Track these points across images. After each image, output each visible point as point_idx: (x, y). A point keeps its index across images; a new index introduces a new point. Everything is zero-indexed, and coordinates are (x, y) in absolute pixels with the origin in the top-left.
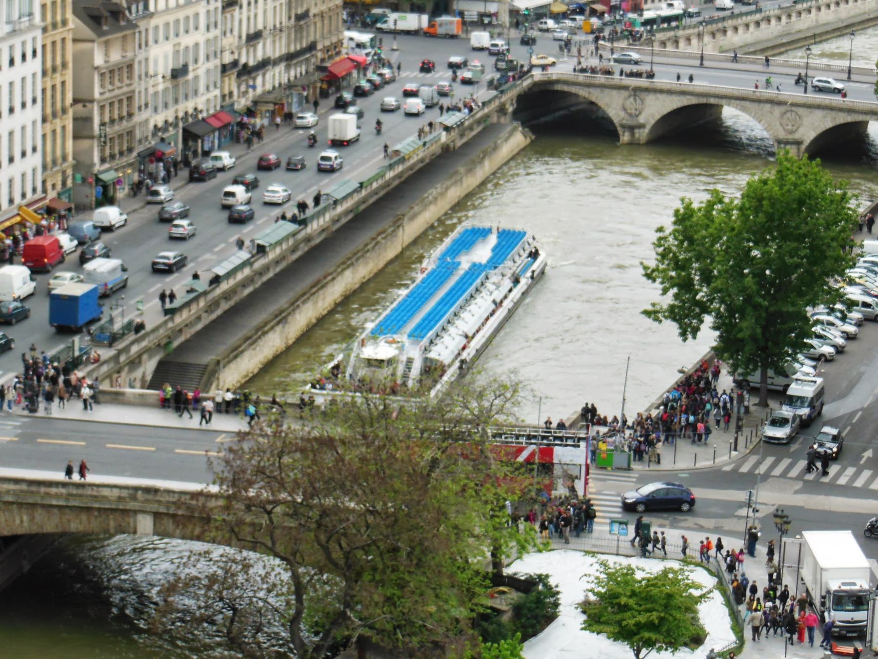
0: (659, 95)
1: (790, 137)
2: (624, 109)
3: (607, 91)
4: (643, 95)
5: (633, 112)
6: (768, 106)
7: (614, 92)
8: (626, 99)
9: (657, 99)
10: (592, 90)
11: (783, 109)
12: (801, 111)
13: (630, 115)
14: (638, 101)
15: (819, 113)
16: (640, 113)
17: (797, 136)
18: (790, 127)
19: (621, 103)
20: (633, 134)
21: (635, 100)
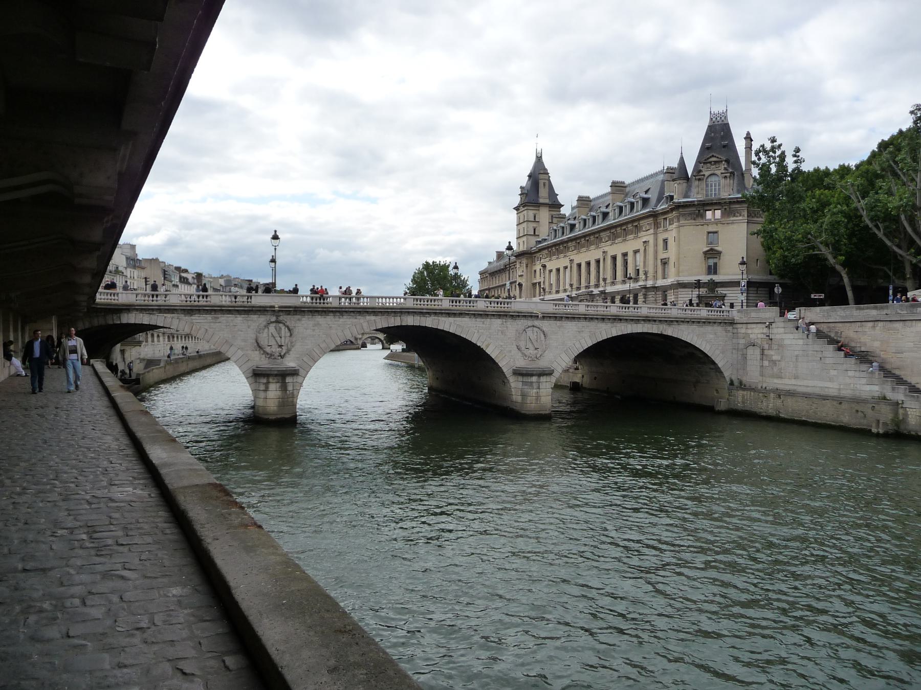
0: (319, 319)
1: (532, 366)
2: (259, 347)
3: (224, 318)
4: (291, 320)
5: (276, 350)
6: (498, 321)
7: (239, 319)
8: (259, 331)
9: (318, 324)
10: (196, 318)
11: (522, 323)
12: (546, 325)
13: (270, 356)
14: (284, 331)
15: (571, 326)
16: (288, 351)
17: (543, 364)
18: (532, 351)
19: (251, 336)
20: (284, 387)
21: (279, 331)
